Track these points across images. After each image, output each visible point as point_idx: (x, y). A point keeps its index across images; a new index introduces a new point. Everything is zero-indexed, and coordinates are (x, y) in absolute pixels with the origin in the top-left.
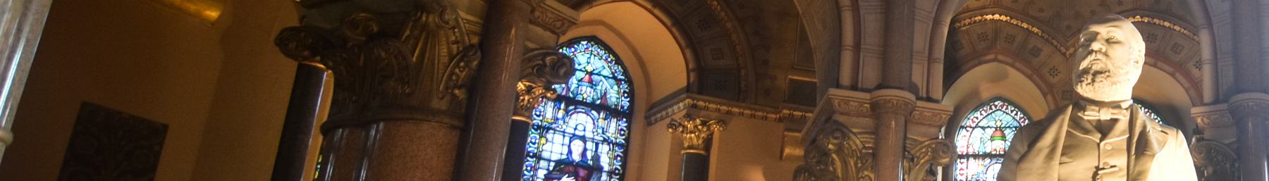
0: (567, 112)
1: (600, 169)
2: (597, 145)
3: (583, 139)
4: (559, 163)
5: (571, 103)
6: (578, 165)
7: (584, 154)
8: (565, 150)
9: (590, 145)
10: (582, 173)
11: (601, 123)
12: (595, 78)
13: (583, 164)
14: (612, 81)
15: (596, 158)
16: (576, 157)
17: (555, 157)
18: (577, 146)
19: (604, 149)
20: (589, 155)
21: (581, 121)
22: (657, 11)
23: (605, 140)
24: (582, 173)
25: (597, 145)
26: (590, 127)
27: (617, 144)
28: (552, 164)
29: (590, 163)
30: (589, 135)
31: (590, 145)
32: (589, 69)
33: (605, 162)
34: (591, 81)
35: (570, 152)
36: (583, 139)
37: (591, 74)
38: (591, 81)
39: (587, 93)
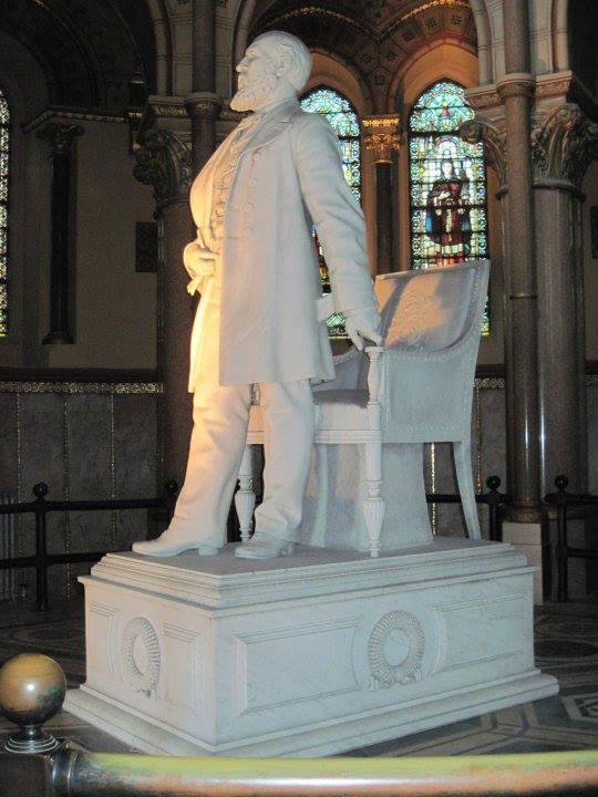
0: (434, 142)
1: (467, 181)
2: (462, 162)
3: (450, 160)
4: (436, 183)
5: (435, 135)
6: (450, 182)
7: (453, 172)
8: (439, 173)
9: (456, 164)
10: (454, 187)
11: (462, 144)
12: (450, 110)
13: (454, 181)
14: (465, 108)
15: (463, 173)
16: (448, 176)
17: (432, 180)
18: (447, 168)
19: (467, 164)
20: (457, 172)
21: (448, 147)
22: (463, 45)
23: (468, 158)
24: (454, 187)
25: (462, 162)
26: (454, 150)
27: (477, 158)
28: (432, 186)
29: (459, 178)
30: (454, 156)
32: (445, 105)
33: (470, 175)
34: (448, 114)
35: (443, 173)
36: (450, 160)
37: (447, 108)
38: (448, 114)
39: (447, 125)
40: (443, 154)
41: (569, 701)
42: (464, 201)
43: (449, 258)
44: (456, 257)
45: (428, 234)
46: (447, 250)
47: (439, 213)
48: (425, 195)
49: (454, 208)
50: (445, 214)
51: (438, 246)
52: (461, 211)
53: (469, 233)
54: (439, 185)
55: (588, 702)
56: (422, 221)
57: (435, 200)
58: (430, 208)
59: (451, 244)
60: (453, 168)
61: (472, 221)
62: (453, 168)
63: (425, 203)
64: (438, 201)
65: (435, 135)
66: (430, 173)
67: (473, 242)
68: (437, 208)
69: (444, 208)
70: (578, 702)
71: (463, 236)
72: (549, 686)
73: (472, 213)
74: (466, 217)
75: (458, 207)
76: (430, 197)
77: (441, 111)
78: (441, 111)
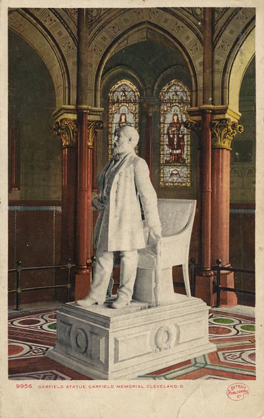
4: (170, 124)
6: (176, 123)
10: (178, 125)
18: (175, 118)
20: (180, 119)
31: (179, 116)
34: (177, 95)
35: (174, 119)
38: (177, 95)
41: (220, 353)
43: (175, 155)
45: (167, 145)
46: (175, 152)
47: (171, 136)
48: (166, 129)
49: (178, 135)
50: (174, 137)
51: (171, 150)
52: (181, 136)
53: (184, 145)
54: (172, 125)
55: (226, 354)
58: (168, 134)
59: (176, 149)
60: (178, 118)
61: (185, 140)
62: (178, 118)
63: (166, 132)
64: (171, 131)
66: (169, 118)
67: (185, 149)
68: (171, 134)
69: (174, 134)
70: (223, 354)
71: (180, 147)
72: (213, 347)
73: (185, 137)
75: (179, 134)
78: (174, 93)
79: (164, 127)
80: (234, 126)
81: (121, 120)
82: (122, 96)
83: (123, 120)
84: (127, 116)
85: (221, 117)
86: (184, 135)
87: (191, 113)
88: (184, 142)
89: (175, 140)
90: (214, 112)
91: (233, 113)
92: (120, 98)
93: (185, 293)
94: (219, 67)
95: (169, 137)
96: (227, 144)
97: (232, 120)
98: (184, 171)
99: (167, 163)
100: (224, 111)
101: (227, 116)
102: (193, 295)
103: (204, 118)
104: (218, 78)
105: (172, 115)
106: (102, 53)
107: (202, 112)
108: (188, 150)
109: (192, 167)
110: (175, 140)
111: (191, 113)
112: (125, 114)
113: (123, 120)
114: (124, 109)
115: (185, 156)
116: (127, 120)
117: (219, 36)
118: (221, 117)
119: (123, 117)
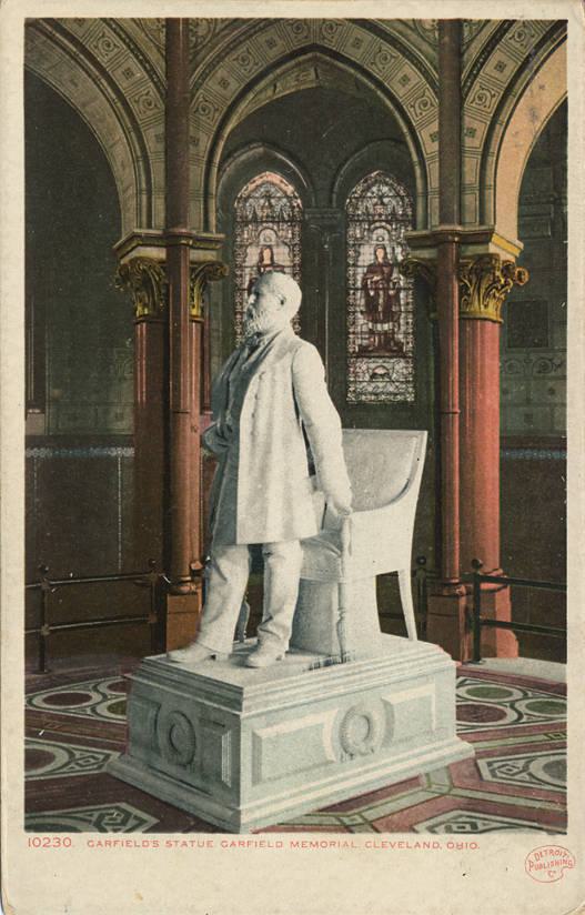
4: (370, 266)
8: (373, 257)
10: (386, 270)
13: (386, 264)
18: (380, 254)
20: (389, 256)
24: (386, 270)
31: (389, 250)
35: (376, 258)
38: (382, 203)
40: (377, 240)
41: (482, 763)
42: (394, 284)
43: (379, 334)
44: (386, 333)
45: (362, 312)
46: (379, 327)
47: (372, 293)
48: (359, 277)
49: (386, 290)
50: (377, 294)
51: (370, 325)
52: (391, 292)
54: (372, 269)
55: (496, 765)
56: (360, 301)
57: (369, 282)
59: (383, 322)
60: (386, 254)
62: (386, 254)
63: (359, 284)
65: (370, 220)
66: (367, 256)
67: (402, 321)
69: (376, 290)
70: (490, 764)
71: (390, 316)
72: (466, 749)
73: (402, 295)
74: (397, 296)
75: (388, 289)
76: (364, 280)
77: (376, 200)
78: (376, 200)
79: (354, 275)
80: (507, 269)
81: (262, 259)
82: (263, 208)
83: (267, 261)
84: (275, 250)
85: (480, 250)
86: (399, 290)
87: (412, 243)
88: (400, 305)
89: (381, 301)
90: (467, 239)
91: (506, 243)
92: (259, 213)
93: (404, 634)
94: (473, 143)
95: (367, 295)
96: (491, 310)
97: (504, 256)
98: (400, 368)
99: (364, 352)
100: (485, 237)
101: (492, 249)
102: (422, 636)
103: (443, 254)
104: (471, 166)
105: (374, 248)
106: (219, 116)
107: (437, 240)
108: (407, 323)
109: (417, 360)
110: (381, 301)
111: (412, 243)
112: (270, 247)
113: (267, 261)
114: (268, 235)
115: (400, 337)
116: (275, 258)
117: (473, 76)
118: (480, 250)
119: (267, 254)
